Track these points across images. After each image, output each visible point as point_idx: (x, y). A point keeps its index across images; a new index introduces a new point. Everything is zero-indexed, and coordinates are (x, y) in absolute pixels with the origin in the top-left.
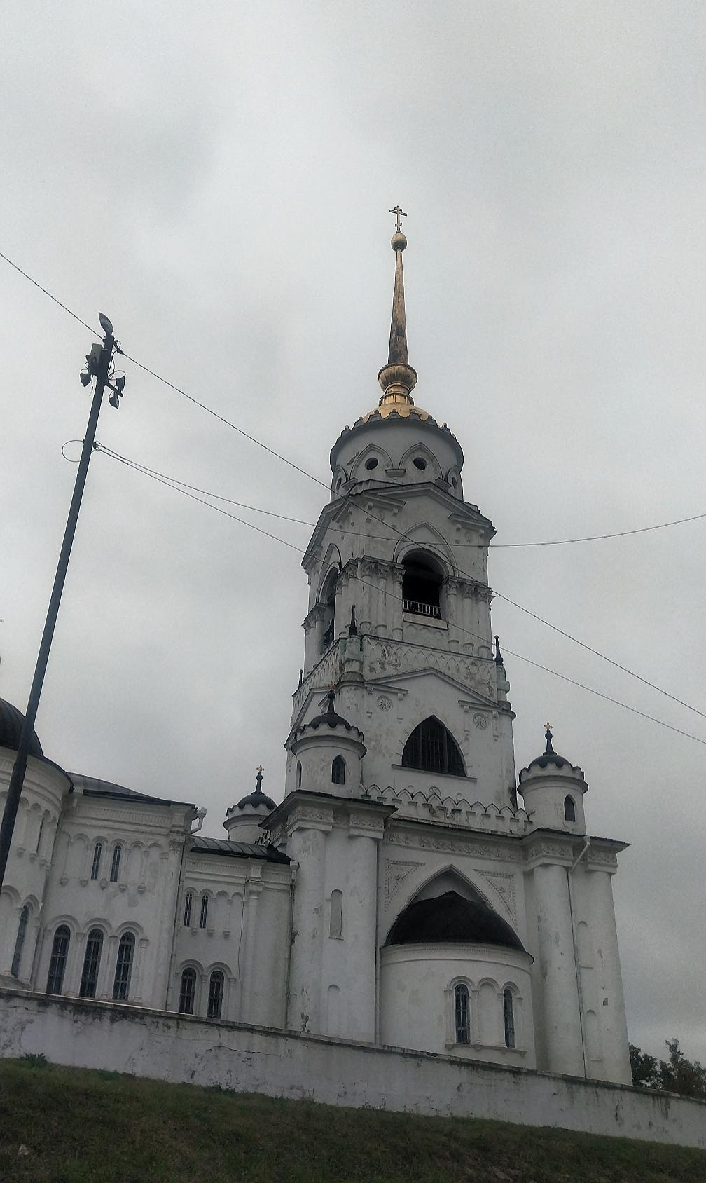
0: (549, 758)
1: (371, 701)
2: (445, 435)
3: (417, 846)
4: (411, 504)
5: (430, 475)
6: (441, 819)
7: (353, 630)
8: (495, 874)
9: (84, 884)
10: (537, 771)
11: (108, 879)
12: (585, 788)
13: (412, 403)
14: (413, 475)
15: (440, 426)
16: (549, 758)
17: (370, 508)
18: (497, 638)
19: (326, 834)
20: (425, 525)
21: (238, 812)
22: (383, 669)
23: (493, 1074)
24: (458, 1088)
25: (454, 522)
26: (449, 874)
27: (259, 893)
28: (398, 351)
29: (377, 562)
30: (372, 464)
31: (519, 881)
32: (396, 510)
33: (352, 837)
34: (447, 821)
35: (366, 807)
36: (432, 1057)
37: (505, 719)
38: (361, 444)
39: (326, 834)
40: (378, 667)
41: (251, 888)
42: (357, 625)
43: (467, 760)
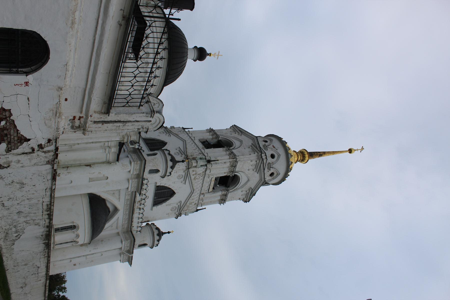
0: (161, 234)
5: (268, 178)
6: (137, 205)
7: (209, 161)
8: (117, 224)
12: (152, 248)
14: (267, 173)
16: (161, 234)
17: (256, 161)
18: (205, 208)
19: (130, 171)
20: (249, 180)
22: (193, 175)
26: (116, 210)
27: (105, 152)
28: (312, 155)
29: (235, 166)
30: (273, 156)
33: (128, 180)
34: (136, 206)
35: (140, 185)
36: (50, 217)
38: (281, 151)
39: (130, 171)
40: (194, 173)
41: (107, 150)
43: (160, 207)
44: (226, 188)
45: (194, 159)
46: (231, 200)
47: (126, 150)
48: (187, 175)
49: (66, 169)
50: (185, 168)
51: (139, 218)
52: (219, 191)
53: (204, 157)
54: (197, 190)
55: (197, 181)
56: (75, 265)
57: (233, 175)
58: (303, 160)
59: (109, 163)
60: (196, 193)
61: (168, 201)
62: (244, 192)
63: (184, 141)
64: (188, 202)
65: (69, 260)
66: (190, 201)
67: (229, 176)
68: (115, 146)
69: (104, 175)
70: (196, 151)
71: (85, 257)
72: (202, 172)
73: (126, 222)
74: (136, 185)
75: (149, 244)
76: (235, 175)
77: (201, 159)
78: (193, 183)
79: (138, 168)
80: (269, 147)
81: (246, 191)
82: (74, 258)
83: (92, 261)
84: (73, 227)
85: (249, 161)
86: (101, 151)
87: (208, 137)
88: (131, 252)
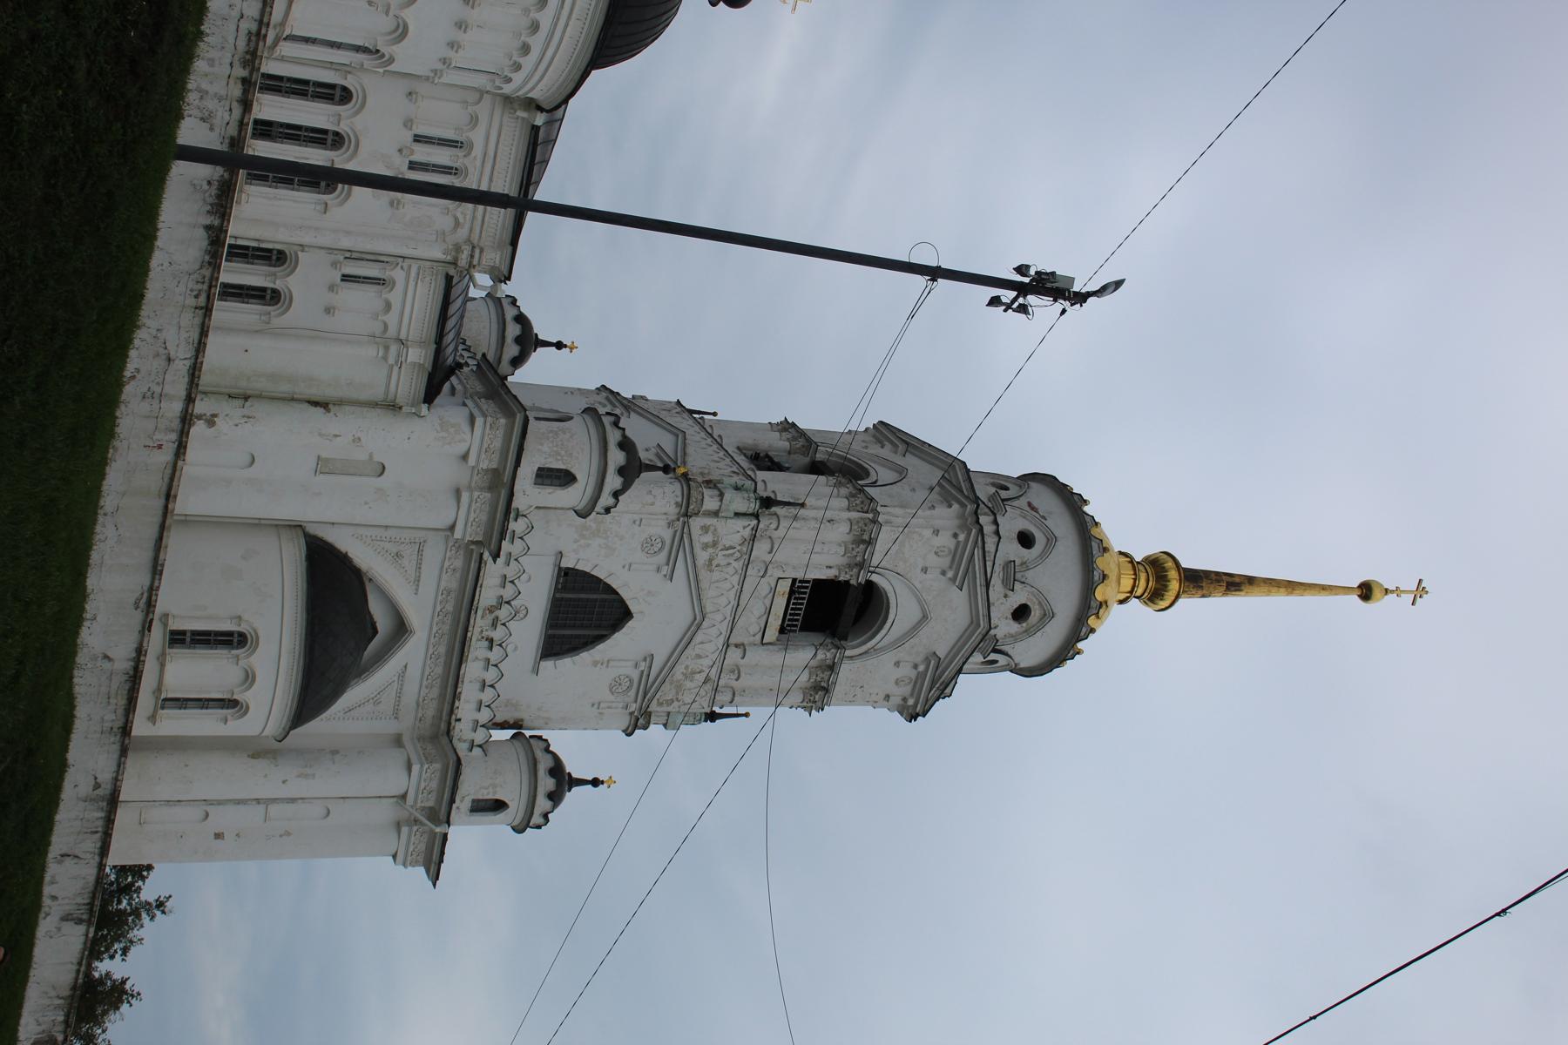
0: (563, 781)
1: (660, 529)
2: (1065, 652)
3: (443, 584)
4: (960, 599)
5: (1004, 627)
6: (480, 623)
7: (768, 503)
8: (399, 696)
9: (408, 123)
10: (545, 763)
11: (413, 158)
12: (519, 829)
13: (1121, 602)
15: (1080, 645)
16: (563, 781)
17: (955, 536)
18: (747, 715)
19: (465, 457)
20: (925, 617)
21: (510, 313)
22: (705, 546)
23: (123, 702)
24: (106, 657)
25: (927, 660)
26: (401, 629)
27: (385, 358)
28: (1199, 581)
29: (870, 542)
30: (1026, 540)
31: (391, 727)
32: (950, 574)
33: (458, 493)
34: (477, 630)
35: (499, 516)
37: (625, 721)
38: (1061, 524)
39: (465, 457)
40: (708, 538)
41: (394, 349)
42: (774, 509)
43: (566, 663)
44: (837, 642)
45: (710, 484)
46: (851, 702)
47: (459, 387)
48: (681, 542)
49: (240, 402)
50: (673, 510)
51: (484, 685)
52: (804, 647)
53: (749, 483)
54: (719, 617)
55: (716, 575)
56: (218, 836)
57: (862, 580)
58: (1154, 596)
59: (393, 407)
60: (714, 632)
61: (601, 647)
62: (906, 671)
63: (677, 433)
64: (679, 669)
65: (198, 812)
66: (687, 661)
67: (847, 582)
68: (421, 344)
69: (371, 456)
70: (721, 465)
71: (262, 808)
72: (737, 539)
73: (435, 692)
74: (484, 517)
75: (513, 805)
76: (870, 584)
77: (737, 488)
78: (703, 585)
79: (498, 444)
80: (1016, 503)
81: (916, 666)
82: (220, 803)
83: (288, 834)
84: (232, 640)
85: (928, 533)
86: (371, 352)
87: (777, 444)
88: (441, 815)
